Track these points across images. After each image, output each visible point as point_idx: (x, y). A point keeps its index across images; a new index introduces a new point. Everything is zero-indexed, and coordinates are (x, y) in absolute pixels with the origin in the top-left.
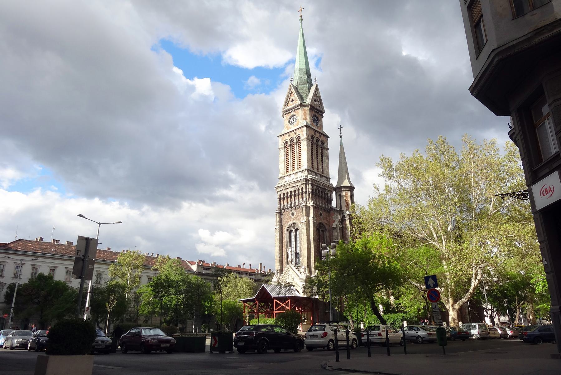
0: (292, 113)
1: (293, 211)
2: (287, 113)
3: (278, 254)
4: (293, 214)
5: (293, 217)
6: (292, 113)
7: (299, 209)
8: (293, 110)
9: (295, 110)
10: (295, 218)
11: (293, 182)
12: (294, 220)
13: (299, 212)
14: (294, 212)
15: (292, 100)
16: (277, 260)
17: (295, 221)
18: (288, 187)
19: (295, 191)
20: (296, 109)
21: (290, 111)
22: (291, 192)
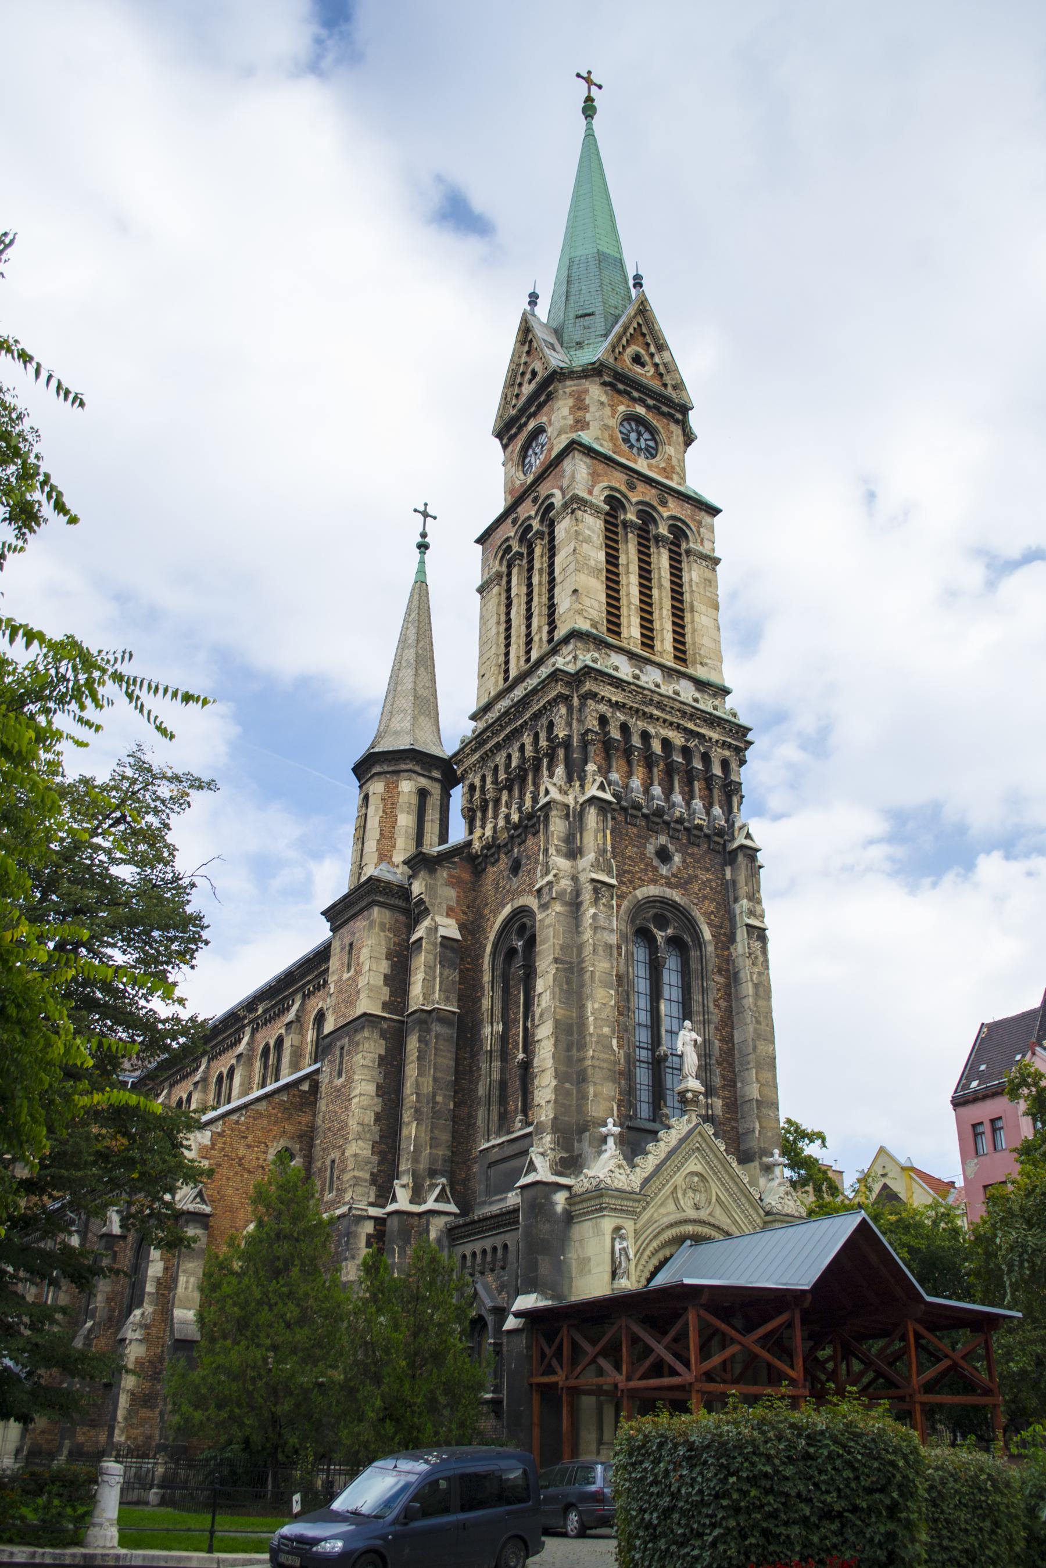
0: (641, 410)
1: (663, 840)
2: (621, 386)
3: (606, 1030)
4: (664, 855)
5: (664, 870)
6: (641, 410)
7: (696, 850)
8: (650, 402)
9: (655, 407)
10: (681, 883)
11: (689, 710)
12: (669, 885)
13: (697, 861)
14: (671, 848)
15: (637, 359)
16: (605, 1065)
17: (676, 895)
18: (656, 712)
19: (686, 751)
20: (665, 409)
21: (636, 394)
22: (666, 743)
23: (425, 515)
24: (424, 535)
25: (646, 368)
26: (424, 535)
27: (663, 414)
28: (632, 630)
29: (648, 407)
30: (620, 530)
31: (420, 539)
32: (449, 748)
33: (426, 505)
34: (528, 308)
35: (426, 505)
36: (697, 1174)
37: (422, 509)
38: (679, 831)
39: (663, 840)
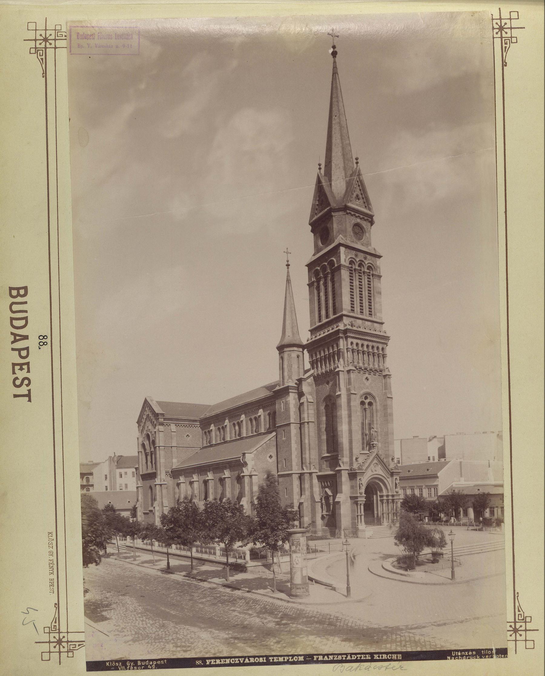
0: (359, 220)
6: (359, 220)
8: (362, 216)
9: (363, 218)
23: (287, 253)
24: (288, 261)
25: (360, 201)
26: (288, 261)
27: (365, 220)
28: (357, 308)
29: (361, 219)
30: (353, 272)
31: (286, 263)
32: (305, 342)
33: (287, 249)
34: (319, 171)
35: (287, 249)
36: (376, 463)
37: (286, 251)
38: (371, 372)
39: (367, 375)
